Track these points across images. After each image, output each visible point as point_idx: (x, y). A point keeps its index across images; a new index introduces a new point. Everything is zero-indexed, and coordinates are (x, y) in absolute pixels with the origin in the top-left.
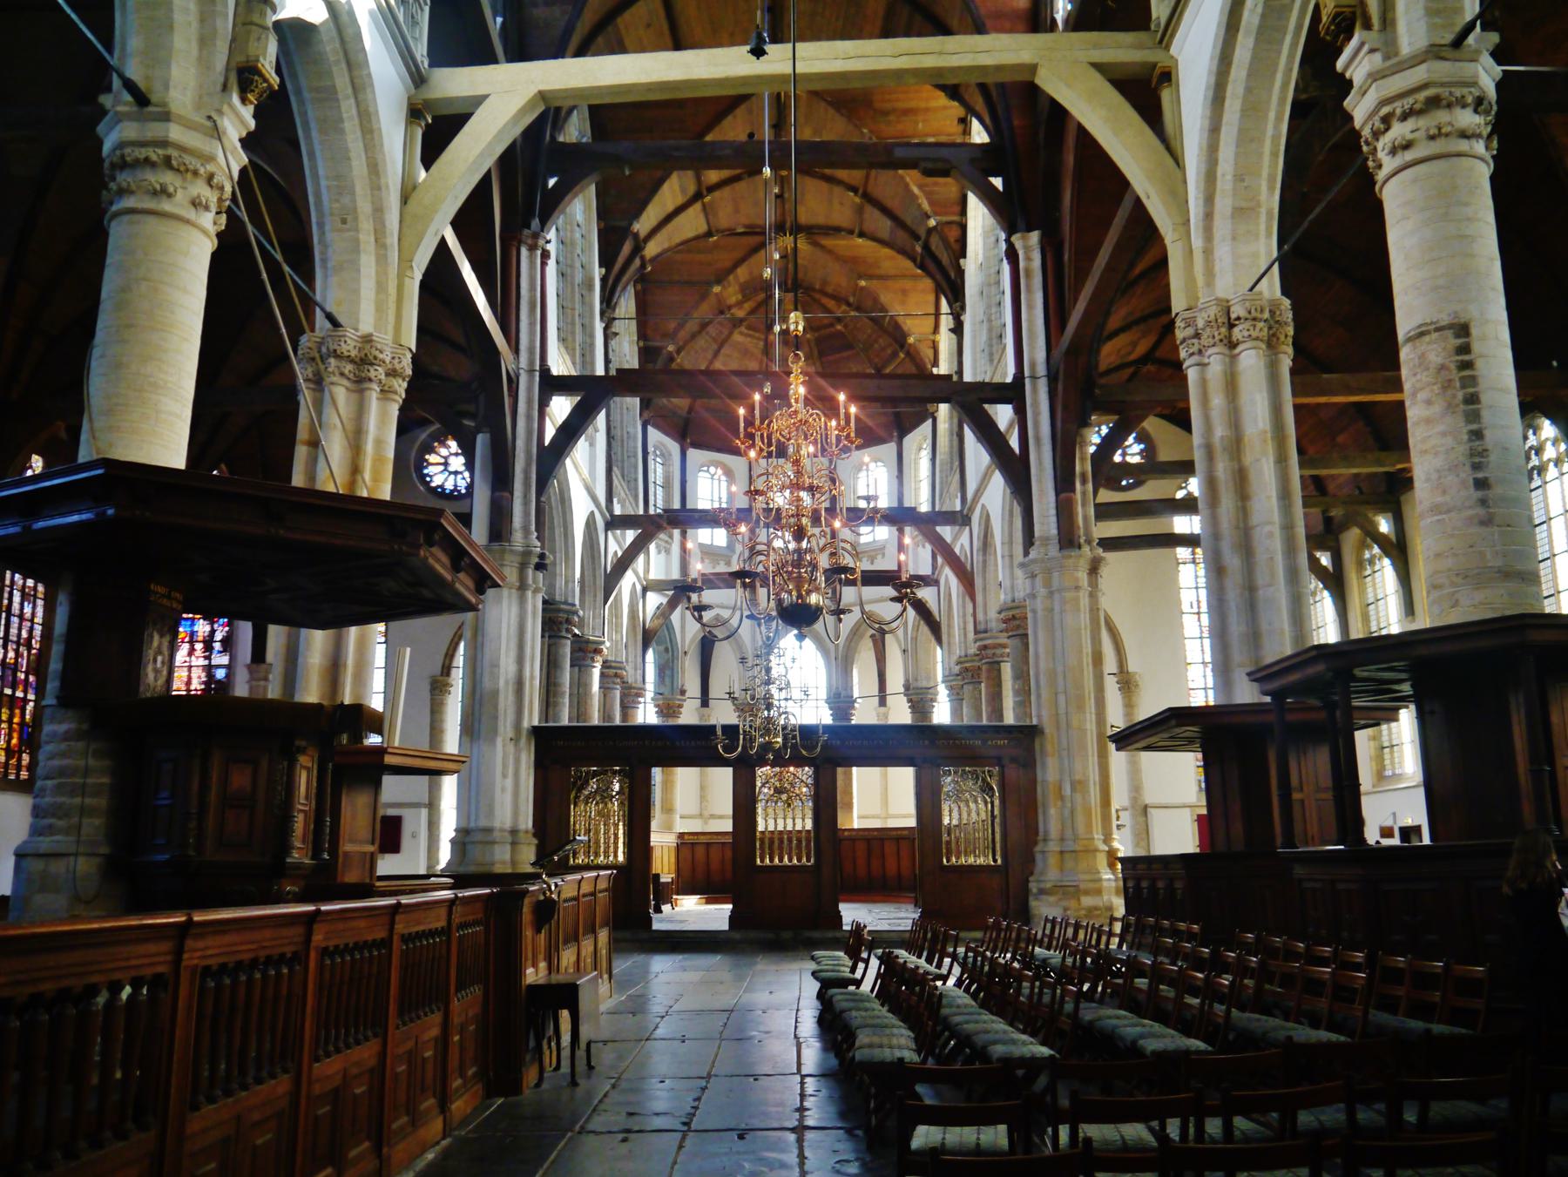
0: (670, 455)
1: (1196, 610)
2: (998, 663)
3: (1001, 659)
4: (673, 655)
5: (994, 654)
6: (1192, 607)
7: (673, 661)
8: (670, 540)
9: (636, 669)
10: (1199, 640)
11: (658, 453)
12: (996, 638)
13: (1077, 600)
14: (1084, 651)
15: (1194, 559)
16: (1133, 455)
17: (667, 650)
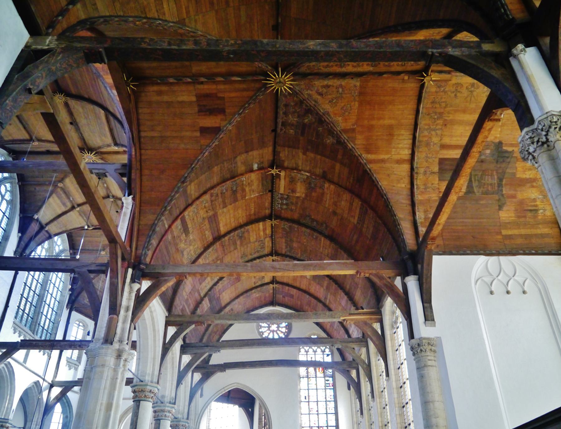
0: (88, 326)
1: (307, 400)
2: (160, 420)
3: (161, 418)
4: (70, 420)
5: (158, 415)
6: (306, 399)
7: (69, 423)
8: (77, 363)
9: (36, 425)
10: (311, 415)
11: (81, 324)
12: (160, 406)
13: (102, 373)
14: (100, 402)
15: (308, 375)
16: (282, 327)
17: (67, 417)
